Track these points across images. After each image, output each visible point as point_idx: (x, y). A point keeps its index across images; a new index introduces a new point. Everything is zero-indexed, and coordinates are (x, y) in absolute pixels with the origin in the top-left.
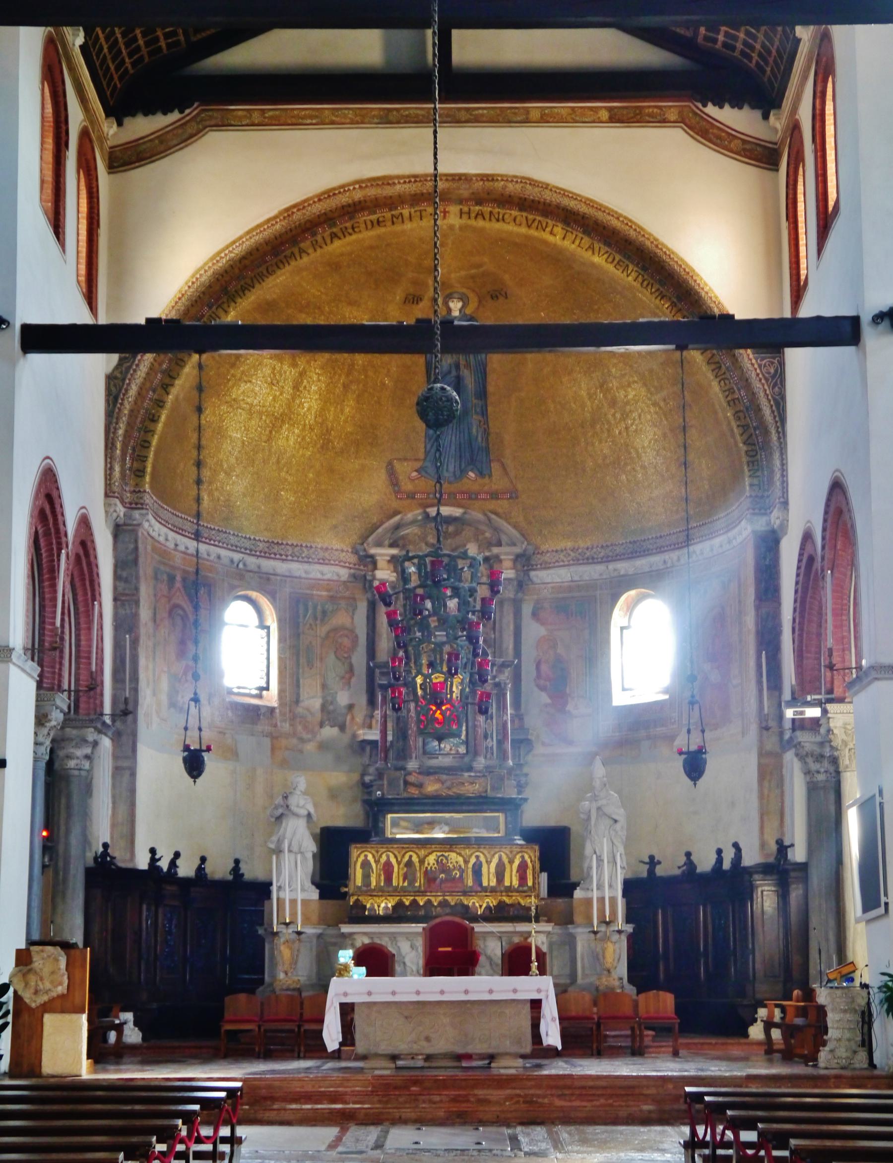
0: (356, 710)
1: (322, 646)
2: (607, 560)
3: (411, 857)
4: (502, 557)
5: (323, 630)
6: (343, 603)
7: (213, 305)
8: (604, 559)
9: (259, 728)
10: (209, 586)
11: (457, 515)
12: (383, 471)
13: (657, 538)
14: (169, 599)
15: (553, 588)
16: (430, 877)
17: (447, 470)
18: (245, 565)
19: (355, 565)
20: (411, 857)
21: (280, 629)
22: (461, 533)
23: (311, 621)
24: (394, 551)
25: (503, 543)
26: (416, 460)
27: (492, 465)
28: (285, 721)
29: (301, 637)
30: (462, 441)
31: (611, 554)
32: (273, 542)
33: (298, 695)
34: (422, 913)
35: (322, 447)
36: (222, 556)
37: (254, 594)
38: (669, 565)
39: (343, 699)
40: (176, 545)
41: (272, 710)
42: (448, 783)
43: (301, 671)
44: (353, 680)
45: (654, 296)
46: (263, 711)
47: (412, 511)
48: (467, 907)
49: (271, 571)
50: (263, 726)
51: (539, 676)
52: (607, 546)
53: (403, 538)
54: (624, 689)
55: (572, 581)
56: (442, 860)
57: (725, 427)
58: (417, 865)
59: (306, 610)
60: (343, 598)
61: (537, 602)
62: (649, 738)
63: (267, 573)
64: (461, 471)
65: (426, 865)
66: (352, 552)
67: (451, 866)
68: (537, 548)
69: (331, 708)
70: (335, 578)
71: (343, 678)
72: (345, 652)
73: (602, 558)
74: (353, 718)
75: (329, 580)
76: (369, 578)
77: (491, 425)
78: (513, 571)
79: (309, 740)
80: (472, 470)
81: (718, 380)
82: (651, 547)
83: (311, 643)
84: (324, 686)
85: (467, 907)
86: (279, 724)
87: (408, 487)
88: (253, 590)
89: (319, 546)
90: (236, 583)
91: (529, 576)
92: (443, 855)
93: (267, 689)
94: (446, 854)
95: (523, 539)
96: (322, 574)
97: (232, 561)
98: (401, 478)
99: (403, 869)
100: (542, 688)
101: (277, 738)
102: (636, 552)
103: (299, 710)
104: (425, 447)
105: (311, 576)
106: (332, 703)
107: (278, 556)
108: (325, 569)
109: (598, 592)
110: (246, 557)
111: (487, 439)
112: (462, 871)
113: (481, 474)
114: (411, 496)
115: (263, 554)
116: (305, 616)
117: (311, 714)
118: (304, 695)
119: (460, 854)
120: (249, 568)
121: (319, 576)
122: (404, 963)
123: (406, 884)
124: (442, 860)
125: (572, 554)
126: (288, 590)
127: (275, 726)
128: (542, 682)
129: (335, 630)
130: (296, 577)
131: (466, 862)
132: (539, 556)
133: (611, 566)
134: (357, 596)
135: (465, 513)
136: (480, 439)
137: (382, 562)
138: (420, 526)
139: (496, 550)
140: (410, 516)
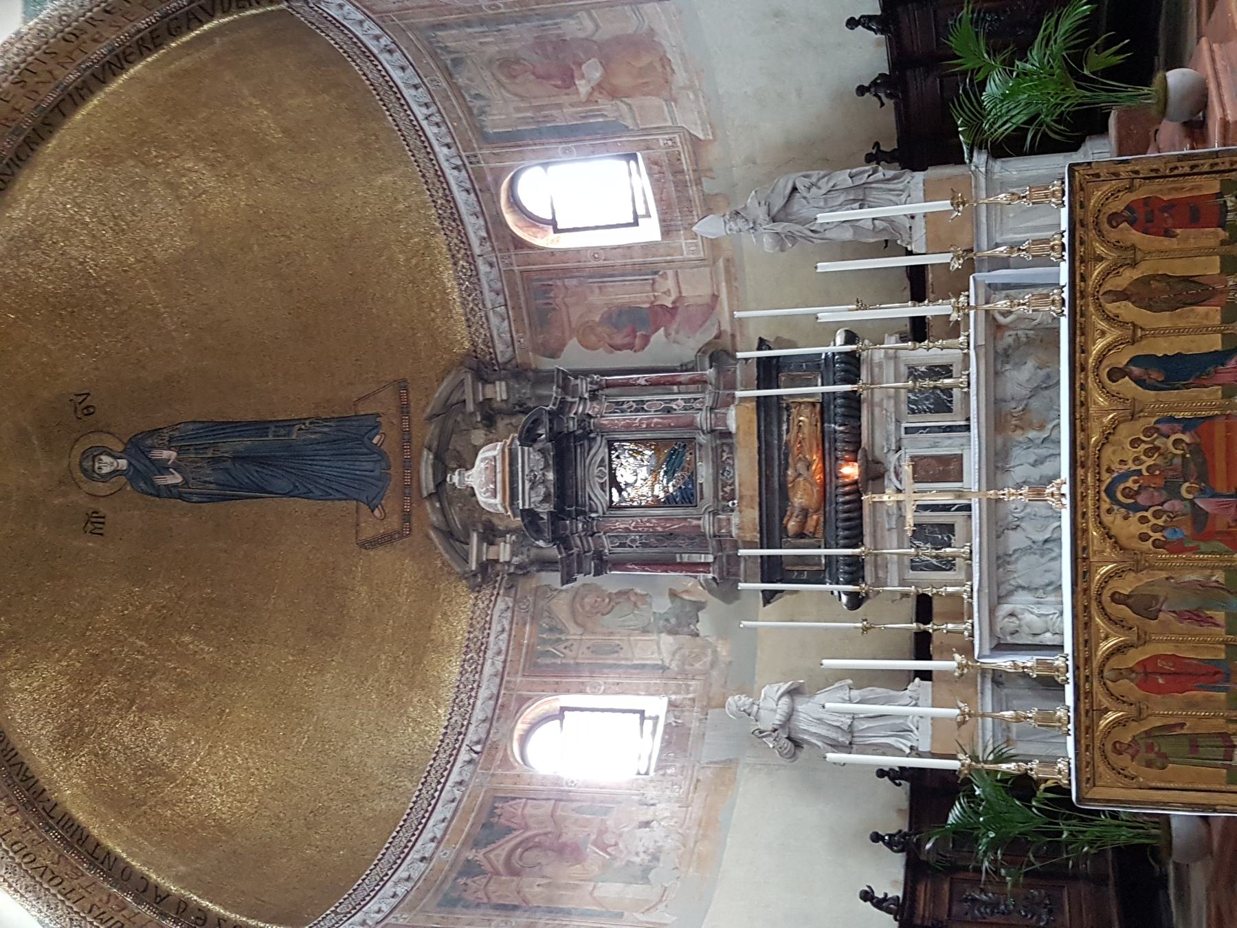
0: (679, 589)
1: (593, 633)
2: (471, 258)
4: (481, 399)
5: (574, 631)
6: (541, 603)
7: (47, 824)
8: (470, 260)
9: (694, 725)
10: (496, 798)
11: (431, 457)
12: (372, 553)
13: (426, 182)
14: (498, 874)
15: (517, 332)
17: (372, 471)
18: (478, 743)
19: (494, 588)
21: (568, 692)
22: (458, 452)
23: (561, 647)
24: (475, 538)
25: (462, 398)
26: (357, 512)
27: (362, 413)
28: (688, 686)
29: (580, 661)
30: (331, 452)
31: (463, 251)
32: (455, 700)
33: (655, 667)
35: (333, 636)
36: (458, 779)
37: (520, 727)
38: (460, 163)
39: (662, 605)
40: (423, 859)
41: (672, 704)
43: (623, 662)
44: (638, 591)
45: (16, 170)
46: (672, 720)
47: (428, 514)
49: (492, 702)
50: (692, 719)
51: (630, 346)
52: (453, 256)
53: (465, 527)
54: (636, 223)
55: (506, 305)
57: (204, 54)
59: (547, 653)
60: (535, 603)
61: (536, 351)
62: (698, 182)
63: (494, 710)
64: (374, 453)
66: (479, 592)
68: (468, 355)
69: (673, 621)
70: (509, 614)
71: (635, 604)
72: (604, 600)
73: (470, 264)
74: (687, 591)
75: (511, 623)
76: (512, 570)
77: (305, 416)
78: (497, 383)
79: (715, 652)
80: (371, 439)
81: (126, 65)
82: (441, 191)
83: (588, 648)
84: (645, 631)
86: (691, 696)
87: (394, 522)
88: (512, 730)
89: (466, 635)
90: (500, 755)
91: (506, 363)
93: (642, 712)
95: (454, 372)
96: (503, 630)
97: (470, 762)
98: (382, 532)
100: (646, 339)
101: (709, 699)
102: (452, 213)
103: (674, 666)
104: (339, 500)
105: (504, 648)
106: (667, 620)
107: (473, 694)
108: (496, 627)
109: (516, 268)
110: (466, 742)
111: (326, 420)
113: (377, 426)
114: (406, 517)
115: (467, 716)
116: (555, 656)
117: (680, 649)
118: (654, 659)
120: (483, 736)
121: (505, 636)
125: (471, 305)
126: (519, 679)
127: (693, 700)
128: (637, 341)
129: (573, 613)
130: (504, 668)
132: (479, 350)
133: (477, 251)
134: (534, 586)
135: (430, 449)
136: (326, 429)
137: (490, 553)
138: (450, 504)
139: (470, 407)
140: (434, 518)
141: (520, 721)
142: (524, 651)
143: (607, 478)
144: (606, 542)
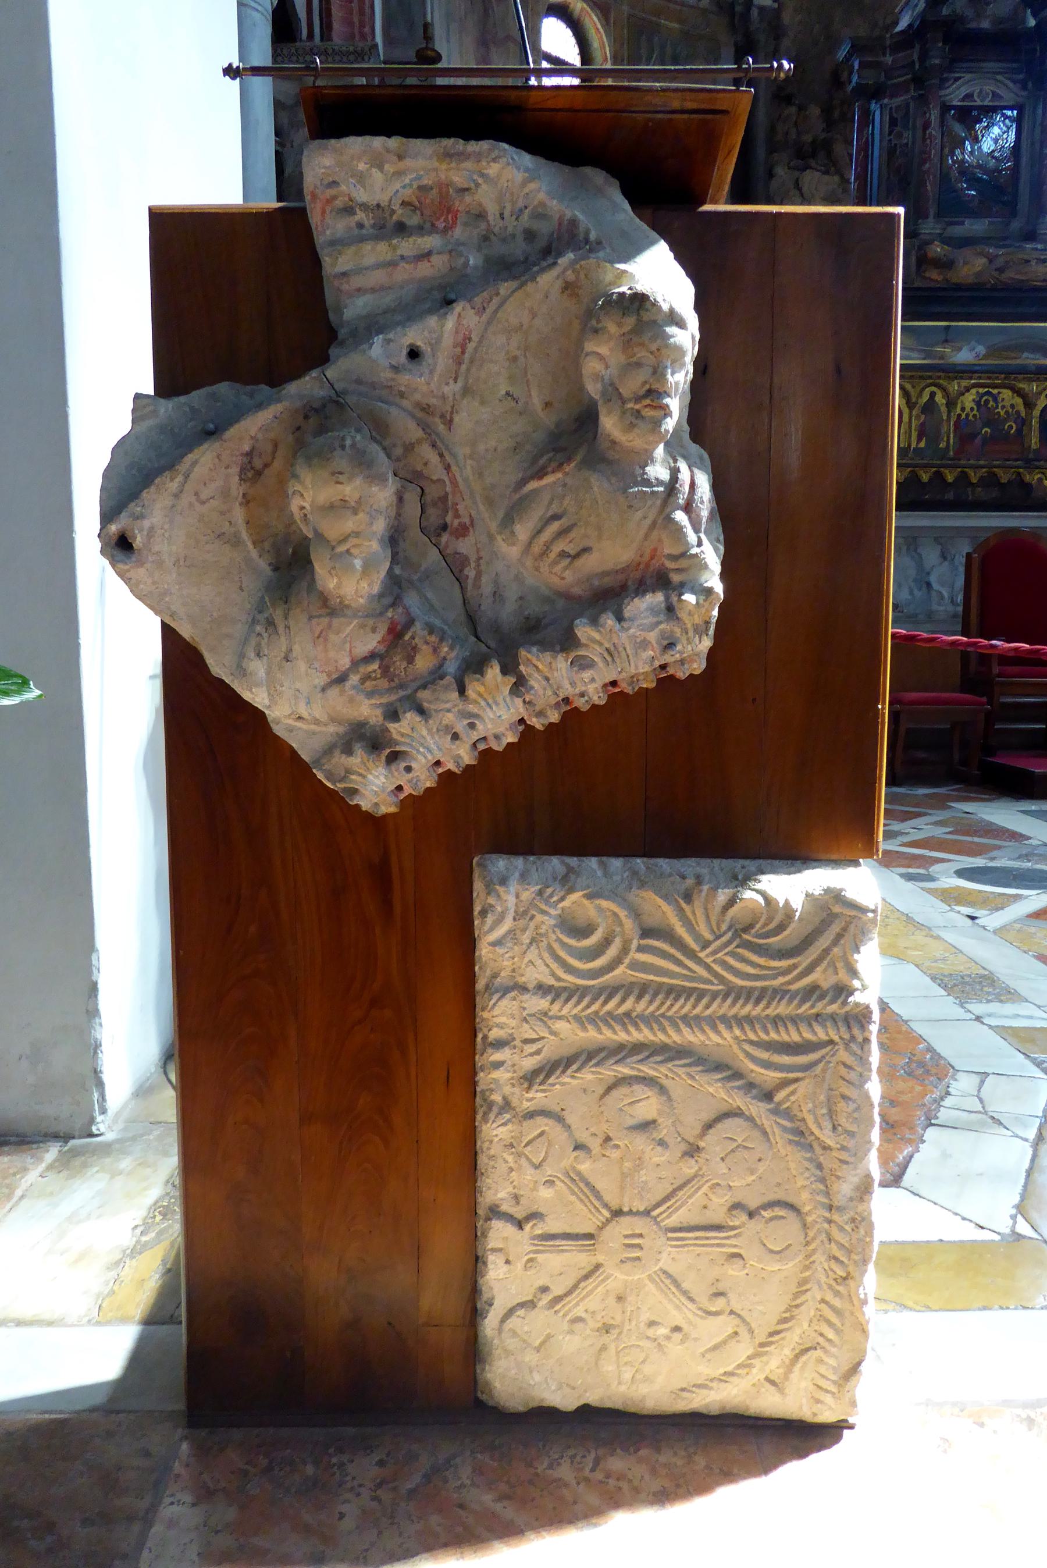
3: (933, 395)
16: (965, 433)
20: (933, 395)
34: (950, 496)
42: (1000, 262)
48: (1027, 487)
56: (987, 402)
58: (943, 409)
65: (958, 411)
67: (1002, 413)
85: (1028, 486)
92: (988, 393)
94: (995, 391)
99: (918, 417)
112: (1023, 423)
119: (1019, 392)
122: (929, 585)
123: (922, 445)
124: (986, 400)
131: (1029, 405)
141: (585, 6)
142: (654, 19)
143: (979, 103)
144: (898, 101)
